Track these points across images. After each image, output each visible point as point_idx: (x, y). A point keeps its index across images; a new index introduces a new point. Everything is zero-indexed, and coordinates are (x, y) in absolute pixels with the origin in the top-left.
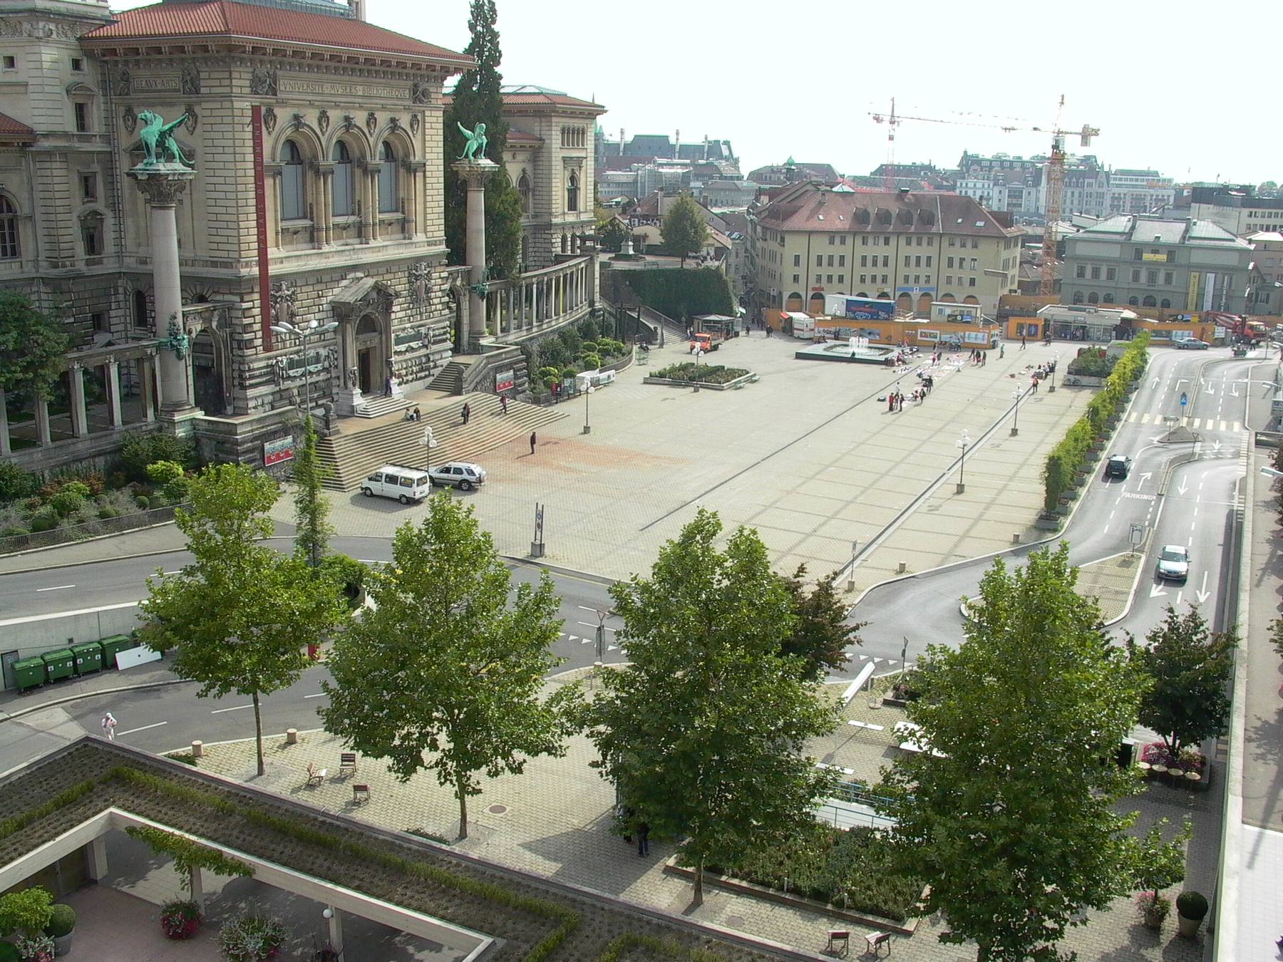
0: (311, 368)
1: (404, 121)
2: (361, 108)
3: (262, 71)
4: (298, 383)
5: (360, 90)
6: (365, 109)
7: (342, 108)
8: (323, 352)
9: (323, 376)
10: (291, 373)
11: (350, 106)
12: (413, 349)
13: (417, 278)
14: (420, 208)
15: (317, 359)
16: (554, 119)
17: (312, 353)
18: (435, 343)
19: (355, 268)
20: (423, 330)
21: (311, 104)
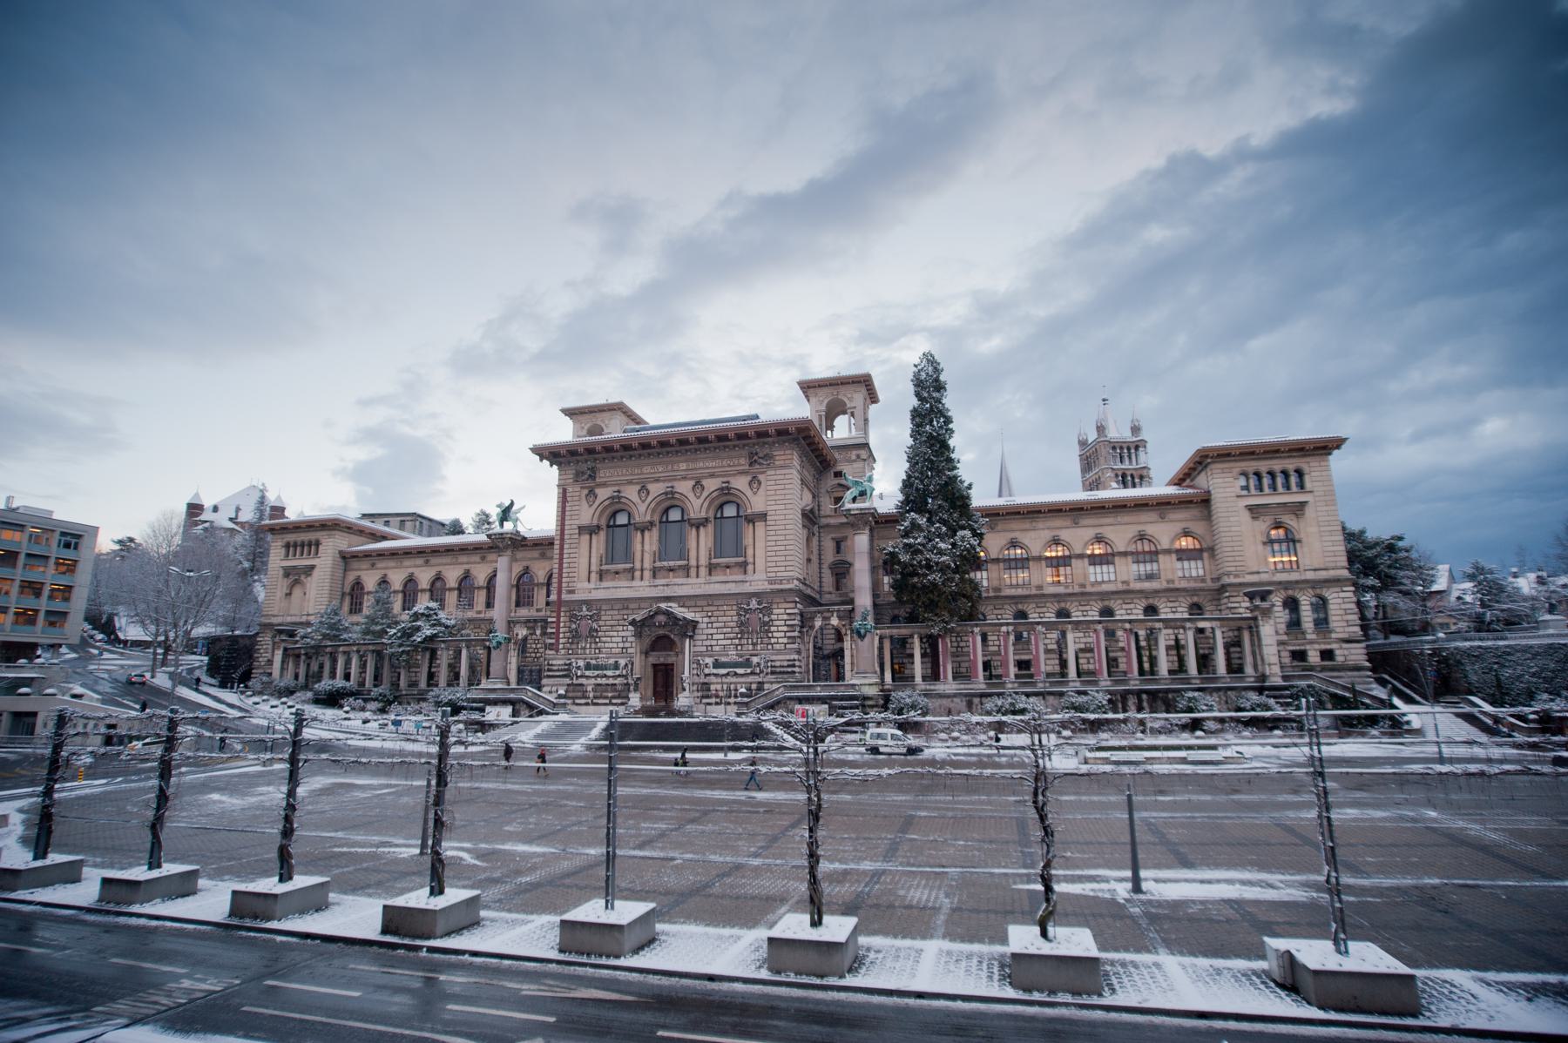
0: (609, 673)
1: (740, 483)
2: (684, 478)
3: (584, 467)
4: (593, 681)
5: (683, 466)
8: (622, 662)
9: (617, 681)
10: (587, 673)
12: (736, 674)
13: (746, 611)
15: (616, 666)
17: (612, 661)
18: (773, 673)
19: (668, 599)
20: (755, 660)
21: (630, 482)
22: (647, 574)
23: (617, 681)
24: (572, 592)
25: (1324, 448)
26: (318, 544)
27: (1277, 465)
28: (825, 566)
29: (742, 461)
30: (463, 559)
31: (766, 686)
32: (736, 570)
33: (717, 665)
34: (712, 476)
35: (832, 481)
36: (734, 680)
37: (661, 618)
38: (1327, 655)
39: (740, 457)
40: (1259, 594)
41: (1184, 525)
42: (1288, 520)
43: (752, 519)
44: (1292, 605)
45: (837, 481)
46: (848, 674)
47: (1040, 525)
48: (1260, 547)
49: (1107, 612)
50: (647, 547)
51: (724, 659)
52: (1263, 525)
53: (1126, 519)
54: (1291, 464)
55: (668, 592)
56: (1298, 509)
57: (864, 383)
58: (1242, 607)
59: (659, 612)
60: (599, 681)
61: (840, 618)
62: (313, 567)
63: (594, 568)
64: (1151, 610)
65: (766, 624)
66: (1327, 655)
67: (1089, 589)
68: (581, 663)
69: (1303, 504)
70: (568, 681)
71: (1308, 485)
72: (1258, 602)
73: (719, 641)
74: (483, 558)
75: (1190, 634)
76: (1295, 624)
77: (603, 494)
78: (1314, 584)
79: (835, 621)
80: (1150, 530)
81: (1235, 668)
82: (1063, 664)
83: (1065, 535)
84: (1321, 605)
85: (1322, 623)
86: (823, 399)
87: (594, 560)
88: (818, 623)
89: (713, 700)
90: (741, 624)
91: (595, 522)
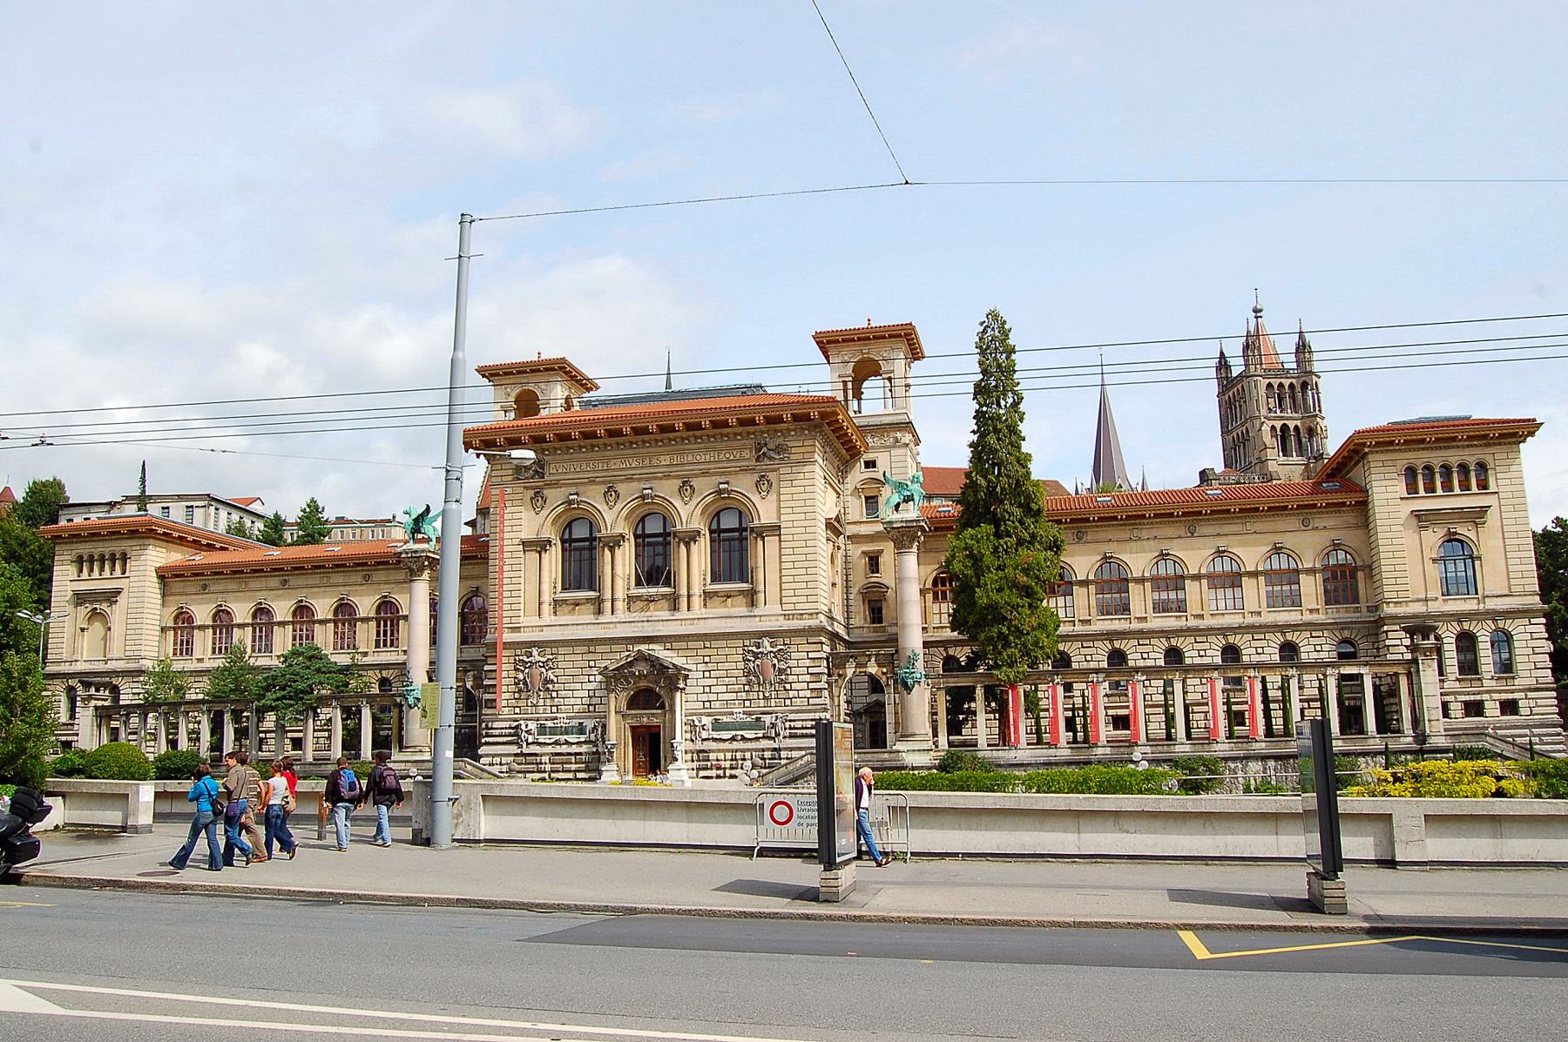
0: (572, 738)
1: (743, 485)
2: (667, 477)
4: (550, 749)
5: (665, 460)
6: (677, 477)
7: (639, 480)
8: (589, 724)
10: (542, 739)
11: (652, 478)
12: (743, 739)
13: (756, 656)
14: (773, 577)
16: (1371, 457)
17: (575, 723)
18: (791, 736)
20: (767, 719)
21: (592, 482)
22: (620, 605)
23: (584, 749)
24: (516, 629)
25: (1515, 433)
26: (125, 558)
27: (1454, 457)
28: (854, 590)
29: (747, 454)
30: (337, 578)
31: (783, 754)
32: (741, 600)
33: (718, 725)
34: (705, 473)
35: (858, 474)
36: (741, 745)
37: (643, 668)
38: (1509, 707)
39: (741, 450)
40: (1420, 628)
41: (1334, 535)
42: (1463, 530)
43: (761, 533)
44: (1467, 642)
45: (870, 473)
46: (890, 737)
47: (1145, 534)
48: (1429, 565)
49: (1231, 653)
50: (619, 569)
51: (725, 719)
52: (1434, 537)
53: (1259, 526)
54: (1471, 457)
55: (649, 630)
56: (1477, 516)
57: (906, 339)
58: (1398, 644)
59: (641, 657)
60: (558, 749)
61: (879, 665)
62: (118, 592)
63: (546, 598)
64: (1289, 651)
65: (781, 671)
66: (1509, 707)
67: (1209, 622)
68: (532, 726)
69: (1483, 511)
70: (514, 749)
71: (1492, 488)
72: (1418, 639)
73: (721, 694)
74: (367, 578)
75: (1332, 684)
76: (1469, 667)
77: (555, 497)
78: (1494, 615)
79: (873, 669)
80: (1288, 541)
81: (1384, 726)
82: (1170, 720)
83: (1178, 550)
84: (1503, 640)
85: (1506, 667)
86: (850, 356)
87: (546, 587)
88: (850, 672)
89: (714, 773)
90: (747, 673)
91: (545, 535)
